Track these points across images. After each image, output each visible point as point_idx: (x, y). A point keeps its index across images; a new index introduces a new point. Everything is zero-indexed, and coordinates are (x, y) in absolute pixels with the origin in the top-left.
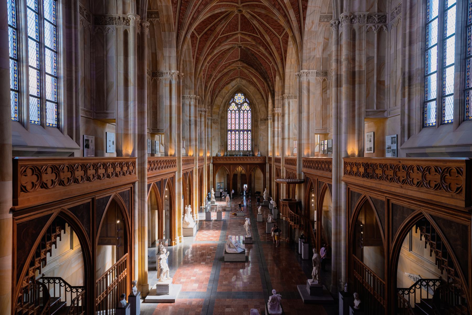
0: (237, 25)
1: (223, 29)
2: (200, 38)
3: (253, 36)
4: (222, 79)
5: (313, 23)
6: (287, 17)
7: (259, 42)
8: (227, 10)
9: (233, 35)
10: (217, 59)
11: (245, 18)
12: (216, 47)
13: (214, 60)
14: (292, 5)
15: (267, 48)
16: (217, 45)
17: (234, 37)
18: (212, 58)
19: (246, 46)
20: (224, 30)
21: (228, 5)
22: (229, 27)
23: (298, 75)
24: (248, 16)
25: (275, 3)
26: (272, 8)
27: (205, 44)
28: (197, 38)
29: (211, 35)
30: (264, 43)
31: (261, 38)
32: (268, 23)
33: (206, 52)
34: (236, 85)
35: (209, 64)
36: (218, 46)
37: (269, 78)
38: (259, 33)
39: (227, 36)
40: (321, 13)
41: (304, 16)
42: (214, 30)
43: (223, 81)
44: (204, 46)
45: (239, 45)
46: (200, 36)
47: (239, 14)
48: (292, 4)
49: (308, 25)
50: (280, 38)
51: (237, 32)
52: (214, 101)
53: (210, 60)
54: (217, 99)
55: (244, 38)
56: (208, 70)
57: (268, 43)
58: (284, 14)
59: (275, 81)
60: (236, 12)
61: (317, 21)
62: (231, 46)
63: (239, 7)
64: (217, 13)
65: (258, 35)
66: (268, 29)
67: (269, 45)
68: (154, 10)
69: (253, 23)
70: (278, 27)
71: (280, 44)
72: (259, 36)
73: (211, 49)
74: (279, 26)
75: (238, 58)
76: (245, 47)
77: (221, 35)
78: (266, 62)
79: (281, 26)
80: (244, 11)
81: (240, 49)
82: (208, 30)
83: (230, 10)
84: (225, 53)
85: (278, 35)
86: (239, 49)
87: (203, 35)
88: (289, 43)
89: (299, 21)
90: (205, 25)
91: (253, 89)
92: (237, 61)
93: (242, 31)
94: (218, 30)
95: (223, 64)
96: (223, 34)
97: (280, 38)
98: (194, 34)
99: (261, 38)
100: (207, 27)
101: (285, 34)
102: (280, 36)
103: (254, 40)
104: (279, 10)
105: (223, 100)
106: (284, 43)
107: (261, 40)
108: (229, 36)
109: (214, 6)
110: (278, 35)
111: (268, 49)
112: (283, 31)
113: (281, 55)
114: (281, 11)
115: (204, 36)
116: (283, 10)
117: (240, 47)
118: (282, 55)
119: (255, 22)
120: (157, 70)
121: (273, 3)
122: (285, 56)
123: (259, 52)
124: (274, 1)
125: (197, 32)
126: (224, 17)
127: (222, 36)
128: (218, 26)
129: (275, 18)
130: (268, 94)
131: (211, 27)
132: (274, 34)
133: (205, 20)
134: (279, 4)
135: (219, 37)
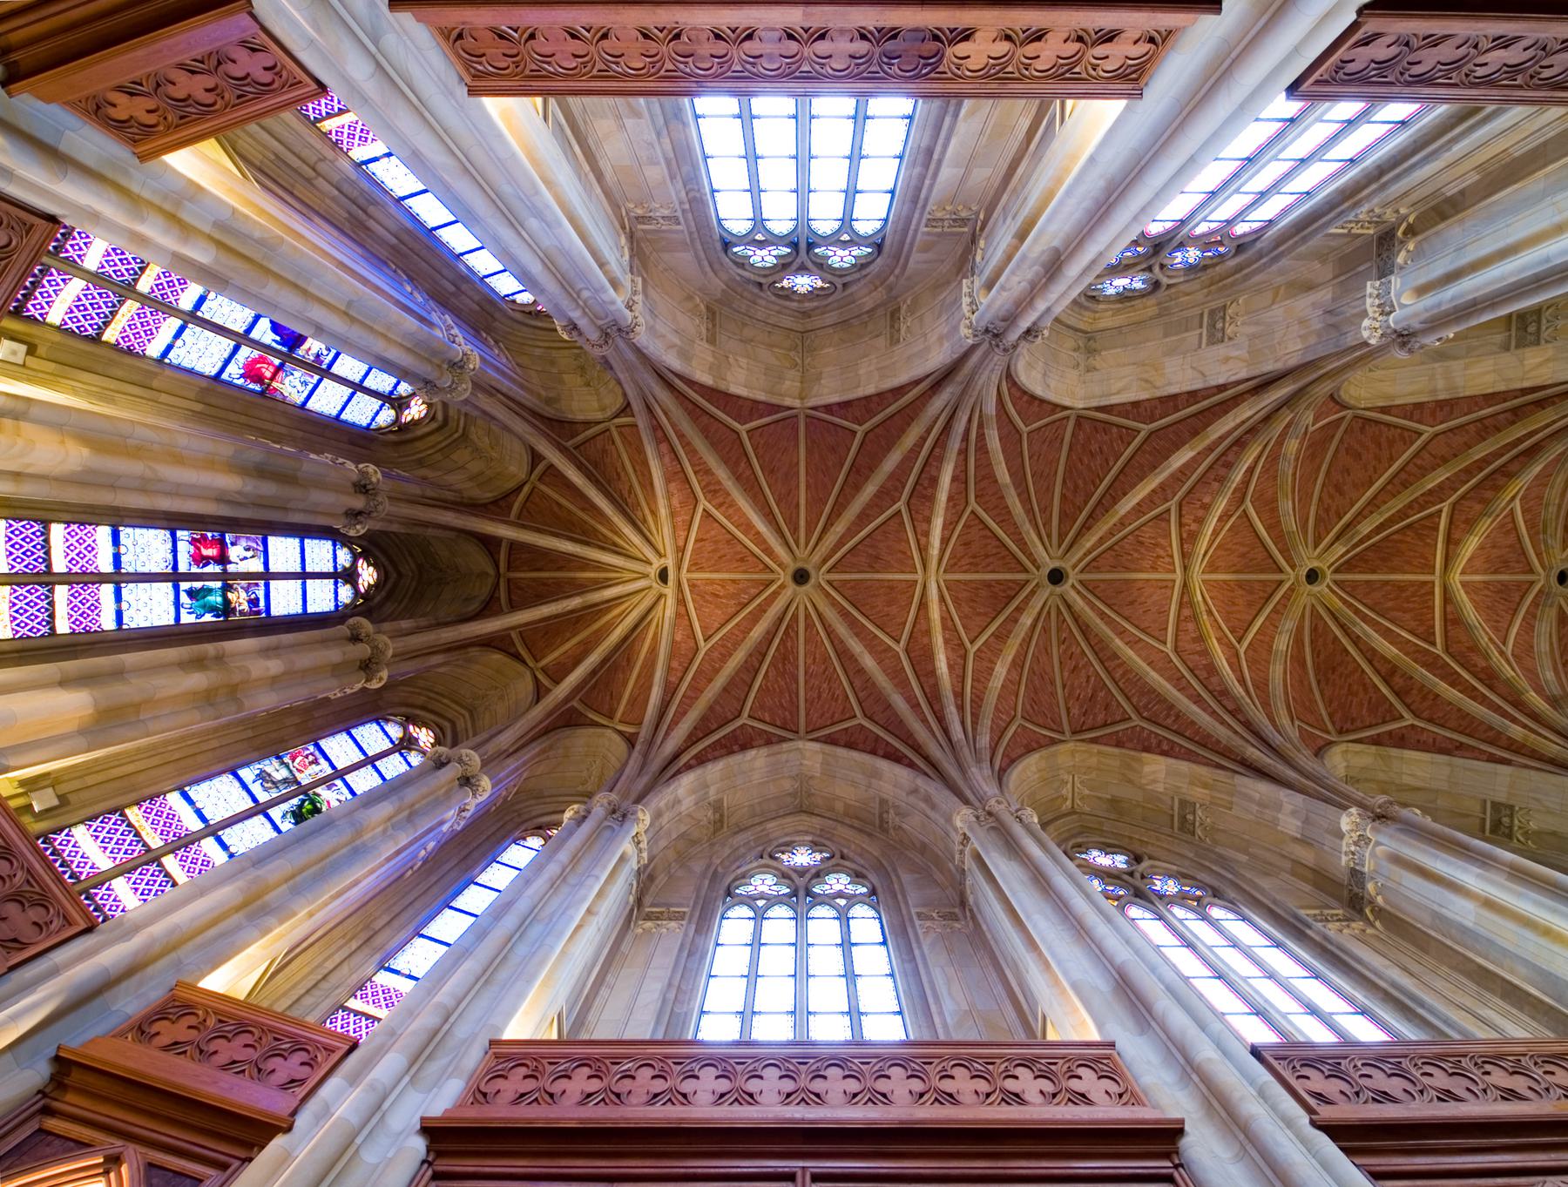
5: (1227, 360)
17: (1462, 596)
22: (1399, 614)
23: (1403, 345)
24: (1340, 549)
25: (1215, 480)
28: (1413, 726)
29: (1412, 678)
32: (1371, 484)
40: (1200, 347)
41: (1215, 391)
42: (1390, 662)
48: (1195, 433)
51: (1437, 584)
58: (1235, 448)
60: (1320, 588)
61: (1221, 350)
85: (1419, 443)
89: (1236, 401)
100: (1375, 686)
101: (1411, 419)
104: (1229, 466)
106: (1452, 413)
107: (1463, 497)
108: (1449, 617)
110: (1419, 443)
112: (1396, 427)
114: (1230, 457)
115: (1409, 701)
116: (1224, 454)
119: (1365, 528)
120: (1340, 885)
121: (1216, 485)
122: (1516, 397)
125: (1384, 722)
126: (1342, 626)
127: (1438, 640)
128: (1374, 650)
131: (1378, 672)
134: (1211, 468)
135: (1439, 650)
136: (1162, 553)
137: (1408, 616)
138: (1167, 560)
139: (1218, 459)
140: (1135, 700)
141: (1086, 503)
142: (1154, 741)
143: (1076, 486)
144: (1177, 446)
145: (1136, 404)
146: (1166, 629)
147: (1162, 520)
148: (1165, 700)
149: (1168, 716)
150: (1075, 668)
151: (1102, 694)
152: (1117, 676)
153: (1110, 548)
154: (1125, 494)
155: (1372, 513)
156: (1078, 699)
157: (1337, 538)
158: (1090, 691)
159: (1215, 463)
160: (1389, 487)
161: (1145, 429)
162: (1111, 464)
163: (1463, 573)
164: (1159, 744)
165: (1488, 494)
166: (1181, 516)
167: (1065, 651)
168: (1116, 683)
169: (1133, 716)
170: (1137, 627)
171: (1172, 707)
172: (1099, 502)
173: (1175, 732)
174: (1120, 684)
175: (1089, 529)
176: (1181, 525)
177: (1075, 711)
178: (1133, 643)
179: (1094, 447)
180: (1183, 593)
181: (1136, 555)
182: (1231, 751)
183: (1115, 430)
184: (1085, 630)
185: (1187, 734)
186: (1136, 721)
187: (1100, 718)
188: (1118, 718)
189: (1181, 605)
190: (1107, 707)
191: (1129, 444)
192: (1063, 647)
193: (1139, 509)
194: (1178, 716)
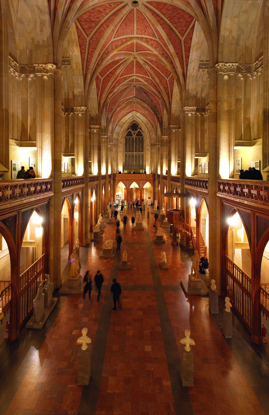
0: (132, 69)
1: (121, 73)
2: (103, 80)
3: (146, 78)
4: (120, 112)
5: (194, 69)
6: (173, 64)
7: (150, 83)
8: (124, 57)
9: (130, 77)
10: (116, 96)
11: (139, 63)
12: (116, 86)
13: (114, 97)
14: (177, 55)
15: (157, 87)
16: (116, 85)
17: (131, 79)
18: (112, 95)
19: (140, 86)
20: (122, 73)
21: (125, 53)
22: (126, 70)
24: (141, 62)
25: (163, 53)
26: (161, 56)
27: (107, 84)
30: (154, 84)
31: (152, 80)
32: (158, 68)
33: (108, 91)
34: (132, 116)
35: (111, 100)
36: (118, 86)
37: (158, 111)
38: (151, 76)
39: (125, 78)
40: (201, 61)
43: (122, 113)
44: (106, 86)
45: (134, 85)
46: (103, 78)
47: (135, 61)
48: (177, 54)
49: (189, 70)
50: (168, 80)
52: (114, 130)
53: (111, 97)
54: (117, 128)
55: (138, 80)
56: (109, 105)
57: (157, 84)
58: (170, 61)
59: (163, 114)
62: (128, 86)
63: (134, 55)
64: (117, 60)
65: (150, 77)
66: (157, 73)
67: (158, 85)
68: (66, 59)
69: (146, 68)
70: (166, 71)
71: (167, 85)
72: (151, 78)
73: (112, 88)
74: (166, 70)
75: (134, 95)
76: (139, 87)
77: (120, 77)
78: (156, 99)
79: (168, 70)
80: (138, 58)
81: (135, 88)
82: (110, 73)
83: (127, 57)
84: (123, 91)
85: (165, 77)
86: (135, 88)
87: (105, 78)
88: (174, 84)
89: (183, 67)
90: (107, 69)
91: (145, 120)
92: (133, 97)
93: (137, 74)
94: (117, 72)
95: (122, 100)
96: (121, 76)
97: (168, 80)
98: (98, 76)
99: (152, 80)
100: (109, 71)
102: (167, 78)
103: (147, 81)
105: (121, 128)
107: (152, 81)
109: (115, 54)
110: (165, 77)
111: (158, 88)
113: (168, 94)
115: (106, 78)
116: (170, 58)
117: (135, 86)
118: (168, 93)
119: (147, 67)
121: (162, 53)
123: (150, 90)
124: (162, 51)
125: (100, 75)
126: (122, 63)
127: (121, 78)
128: (117, 70)
129: (163, 64)
130: (158, 124)
131: (112, 71)
132: (163, 76)
133: (107, 65)
134: (167, 53)
136: (143, 32)
137: (126, 72)
138: (140, 33)
139: (168, 56)
140: (94, 36)
141: (162, 13)
142: (84, 47)
143: (169, 10)
144: (175, 48)
145: (191, 39)
146: (118, 37)
147: (153, 35)
148: (97, 47)
149: (92, 49)
150: (101, 12)
151: (94, 24)
152: (101, 29)
153: (145, 18)
154: (163, 28)
155: (151, 68)
156: (90, 16)
157: (145, 61)
158: (94, 20)
159: (167, 54)
160: (156, 71)
161: (183, 39)
162: (174, 25)
163: (136, 79)
164: (83, 49)
165: (152, 85)
166: (154, 40)
167: (106, 7)
168: (99, 29)
169: (89, 37)
170: (118, 29)
171: (95, 49)
172: (162, 19)
173: (88, 52)
174: (99, 30)
175: (153, 14)
176: (151, 40)
177: (85, 16)
178: (113, 31)
179: (181, 20)
180: (130, 38)
181: (142, 25)
182: (88, 70)
183: (185, 29)
184: (115, 14)
185: (89, 56)
186: (88, 39)
187: (86, 27)
188: (87, 33)
189: (126, 38)
190: (90, 28)
191: (179, 33)
192: (108, 6)
193: (157, 31)
194: (93, 52)
